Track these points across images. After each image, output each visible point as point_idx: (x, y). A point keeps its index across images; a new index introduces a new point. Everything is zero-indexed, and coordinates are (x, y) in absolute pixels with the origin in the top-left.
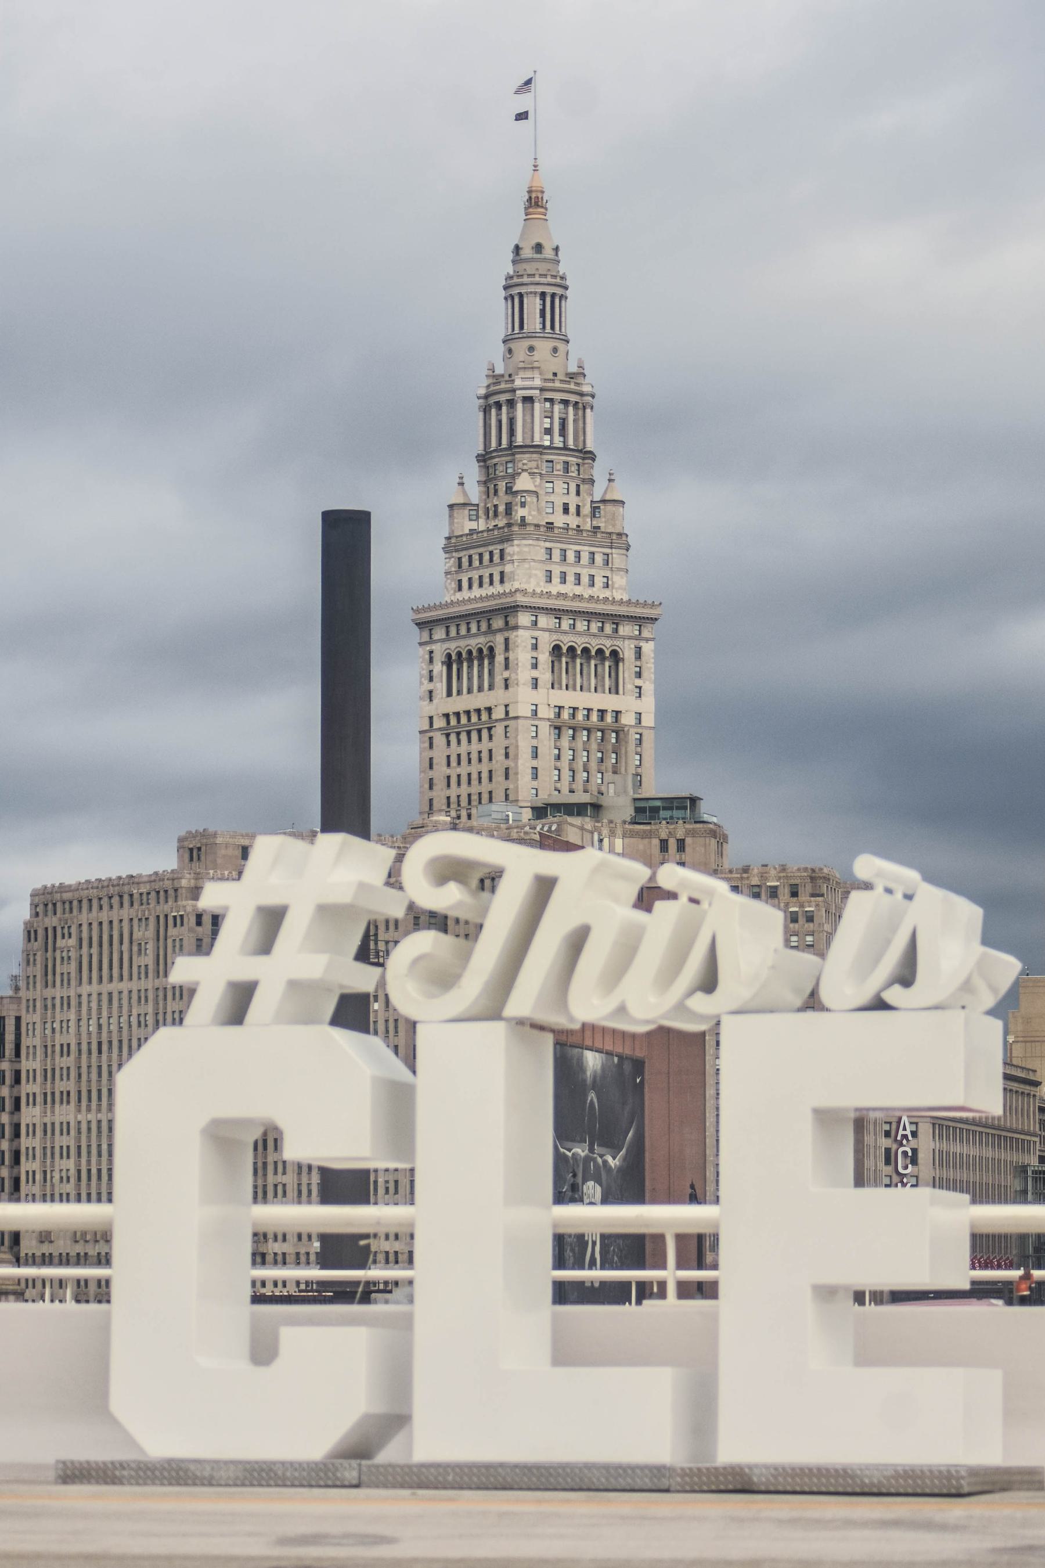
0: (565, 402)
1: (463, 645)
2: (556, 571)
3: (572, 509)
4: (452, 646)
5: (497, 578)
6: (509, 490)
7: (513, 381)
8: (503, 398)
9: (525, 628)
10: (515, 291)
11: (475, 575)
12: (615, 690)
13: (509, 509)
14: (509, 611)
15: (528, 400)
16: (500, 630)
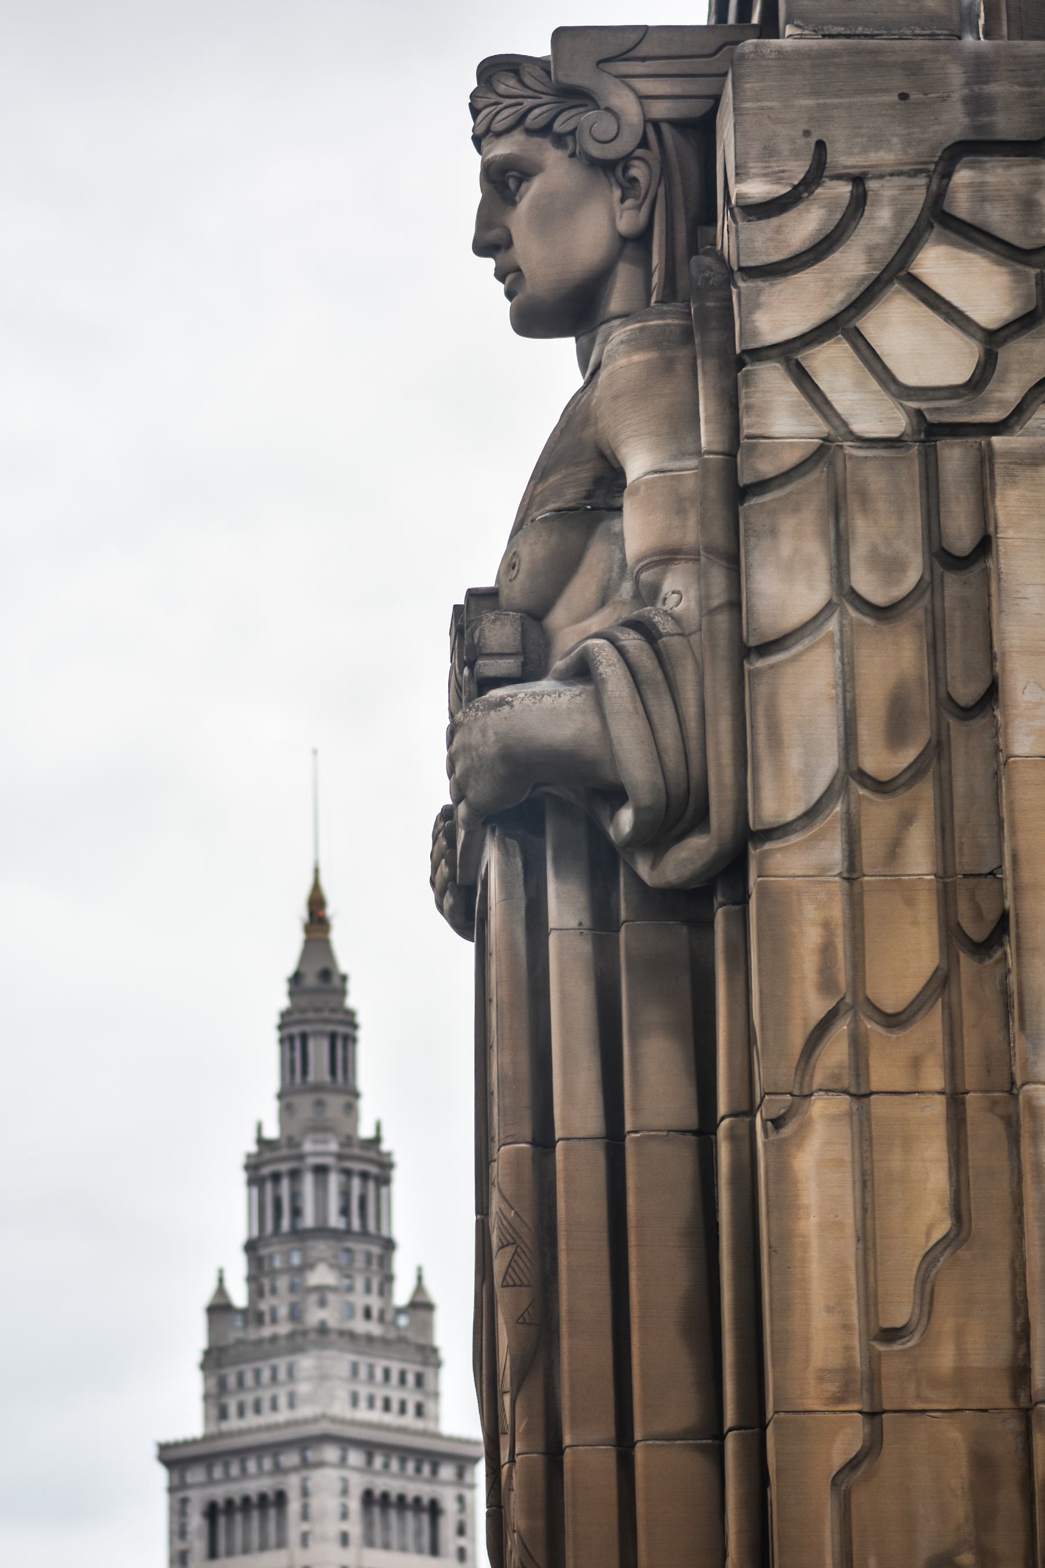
0: (365, 1176)
1: (236, 1490)
2: (363, 1391)
3: (375, 1313)
4: (219, 1493)
5: (283, 1401)
6: (293, 1288)
7: (298, 1145)
8: (284, 1167)
9: (333, 1466)
10: (296, 1030)
11: (249, 1398)
12: (435, 1550)
13: (296, 1314)
14: (306, 1444)
15: (321, 1171)
16: (295, 1469)
